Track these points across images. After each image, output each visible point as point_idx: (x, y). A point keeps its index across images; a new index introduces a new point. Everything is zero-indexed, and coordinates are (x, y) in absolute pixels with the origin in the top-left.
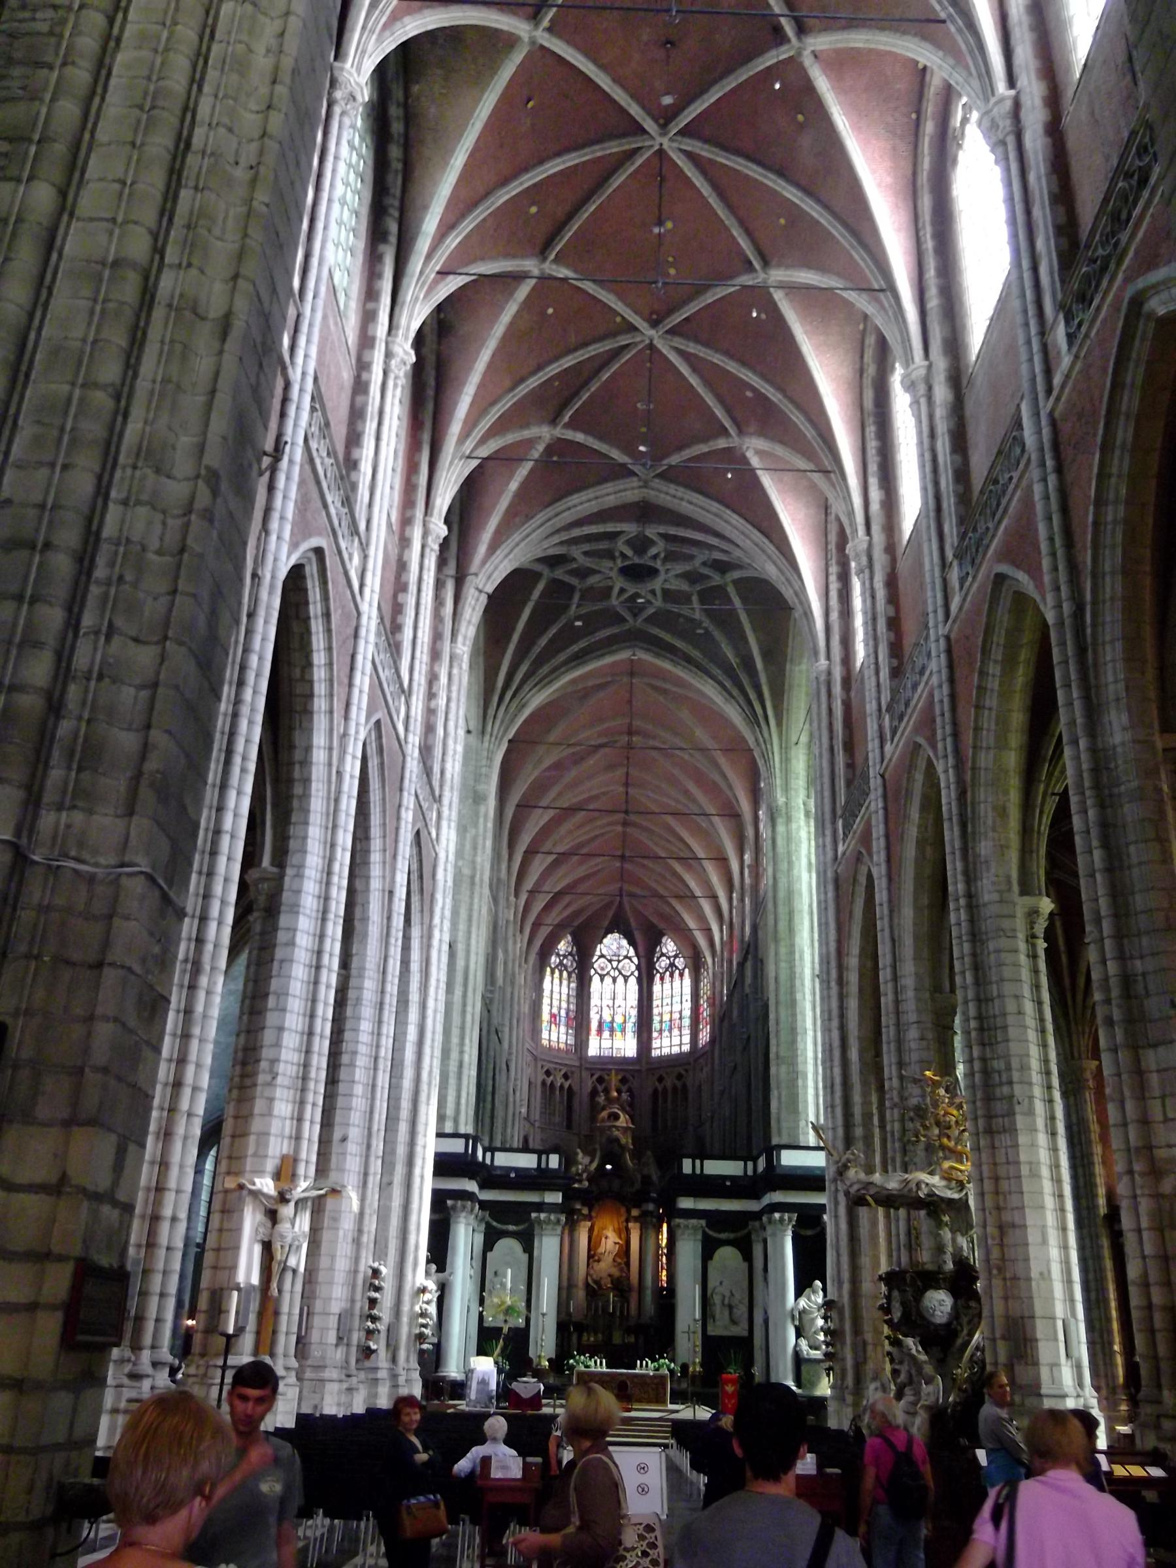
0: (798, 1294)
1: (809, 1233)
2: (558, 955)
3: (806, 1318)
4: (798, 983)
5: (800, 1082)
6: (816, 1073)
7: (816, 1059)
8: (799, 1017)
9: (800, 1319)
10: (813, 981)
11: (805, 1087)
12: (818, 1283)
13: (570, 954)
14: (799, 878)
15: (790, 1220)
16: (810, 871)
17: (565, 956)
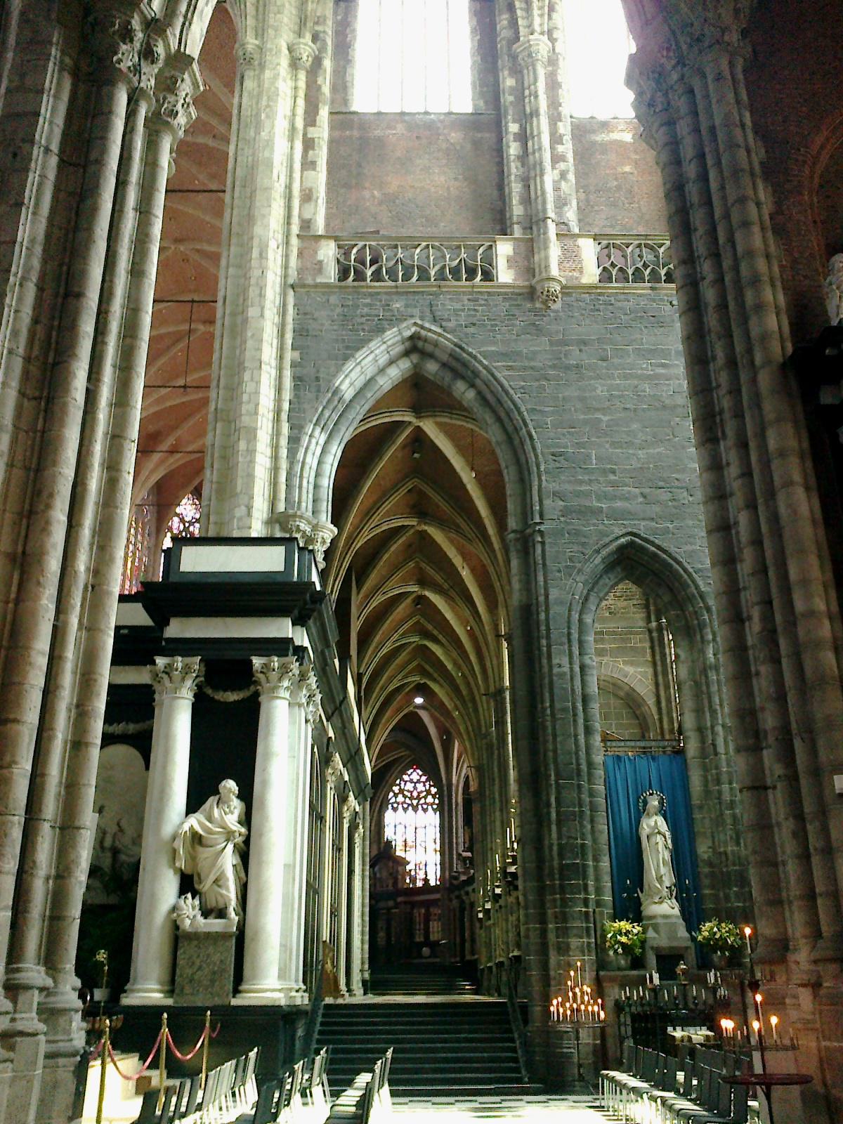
0: (193, 806)
1: (232, 697)
2: (182, 520)
3: (204, 853)
4: (253, 292)
5: (242, 445)
6: (277, 433)
7: (278, 412)
8: (250, 344)
9: (193, 858)
10: (284, 295)
11: (251, 452)
12: (230, 785)
13: (198, 521)
14: (269, 144)
15: (187, 670)
16: (291, 139)
17: (191, 523)
